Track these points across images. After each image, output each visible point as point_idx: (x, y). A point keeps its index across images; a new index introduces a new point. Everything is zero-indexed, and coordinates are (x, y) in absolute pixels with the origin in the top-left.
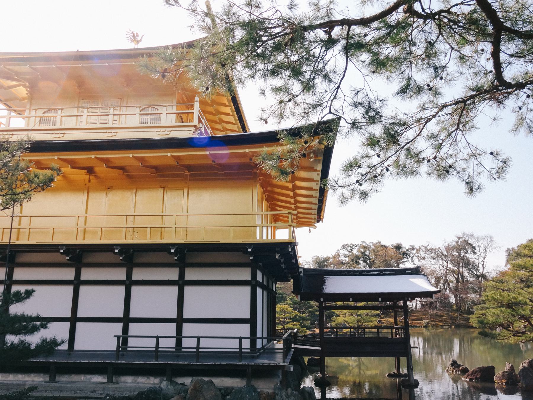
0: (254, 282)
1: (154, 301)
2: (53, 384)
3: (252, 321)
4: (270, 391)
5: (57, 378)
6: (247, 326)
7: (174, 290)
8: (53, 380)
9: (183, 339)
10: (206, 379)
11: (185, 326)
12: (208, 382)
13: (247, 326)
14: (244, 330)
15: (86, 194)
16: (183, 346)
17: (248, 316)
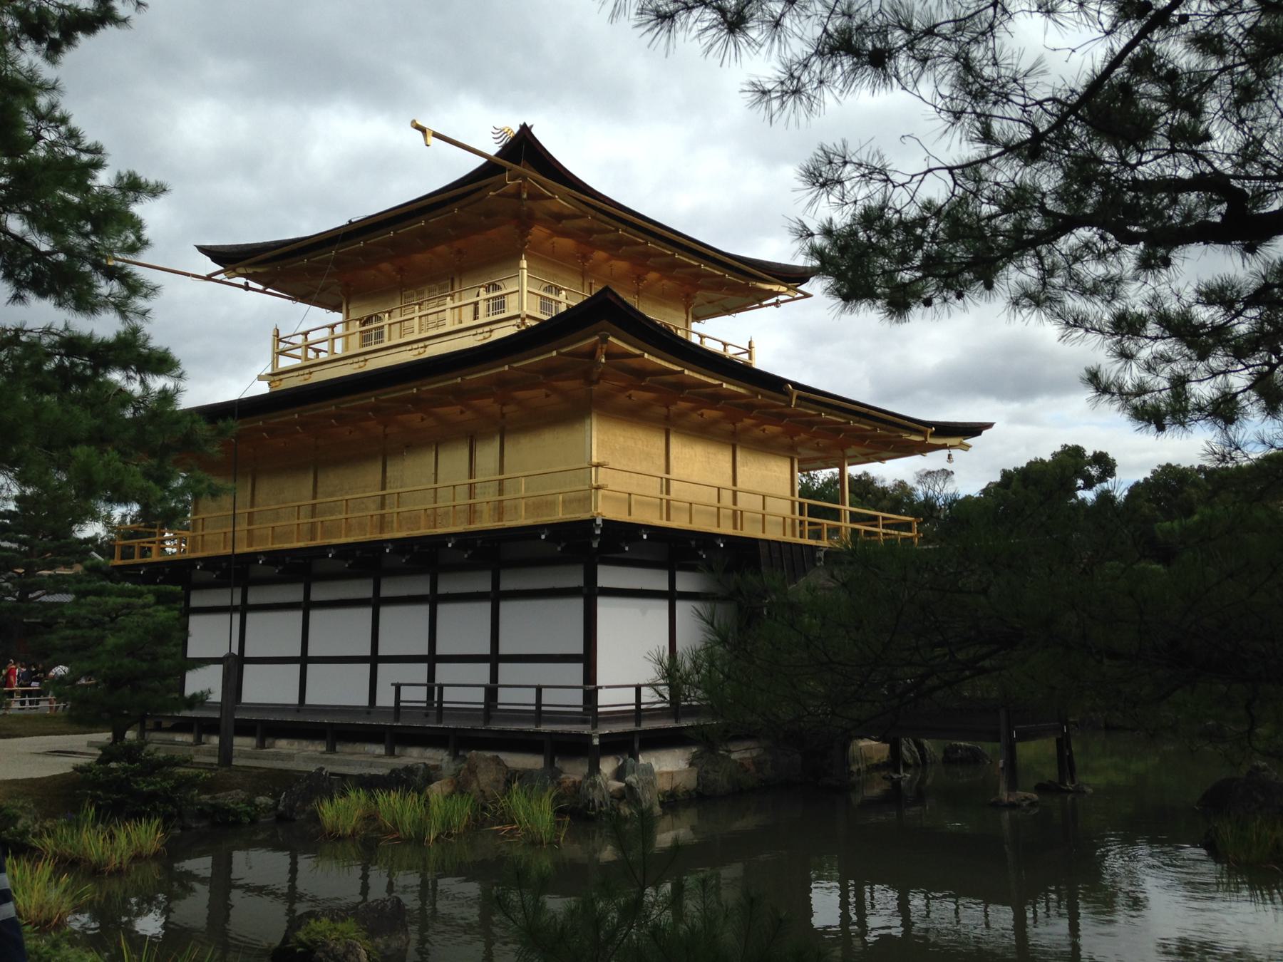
0: (585, 591)
1: (464, 627)
2: (335, 757)
3: (588, 658)
4: (578, 778)
5: (338, 748)
6: (579, 668)
7: (486, 607)
8: (331, 749)
9: (500, 690)
10: (488, 754)
11: (503, 668)
12: (486, 759)
13: (579, 668)
14: (575, 672)
15: (497, 444)
16: (500, 701)
17: (579, 650)
